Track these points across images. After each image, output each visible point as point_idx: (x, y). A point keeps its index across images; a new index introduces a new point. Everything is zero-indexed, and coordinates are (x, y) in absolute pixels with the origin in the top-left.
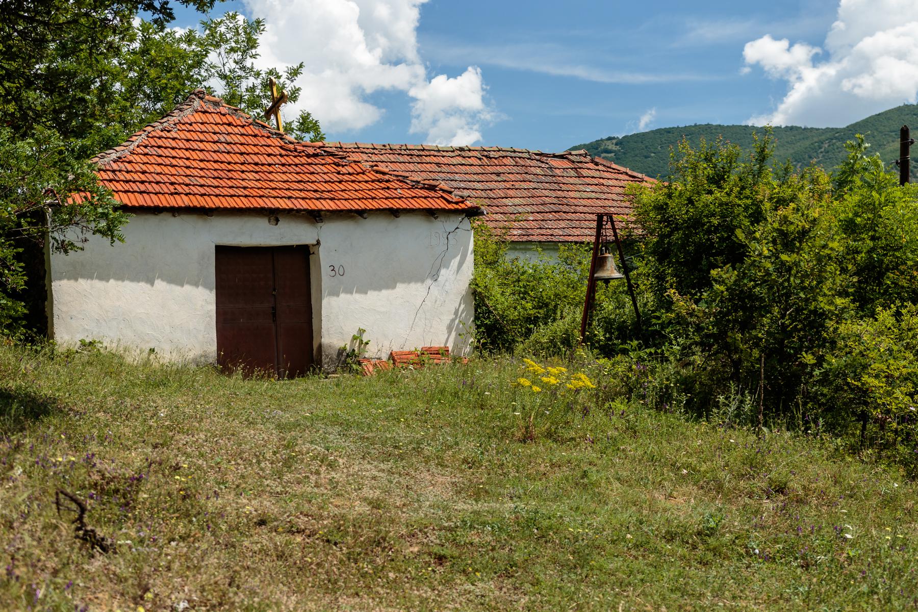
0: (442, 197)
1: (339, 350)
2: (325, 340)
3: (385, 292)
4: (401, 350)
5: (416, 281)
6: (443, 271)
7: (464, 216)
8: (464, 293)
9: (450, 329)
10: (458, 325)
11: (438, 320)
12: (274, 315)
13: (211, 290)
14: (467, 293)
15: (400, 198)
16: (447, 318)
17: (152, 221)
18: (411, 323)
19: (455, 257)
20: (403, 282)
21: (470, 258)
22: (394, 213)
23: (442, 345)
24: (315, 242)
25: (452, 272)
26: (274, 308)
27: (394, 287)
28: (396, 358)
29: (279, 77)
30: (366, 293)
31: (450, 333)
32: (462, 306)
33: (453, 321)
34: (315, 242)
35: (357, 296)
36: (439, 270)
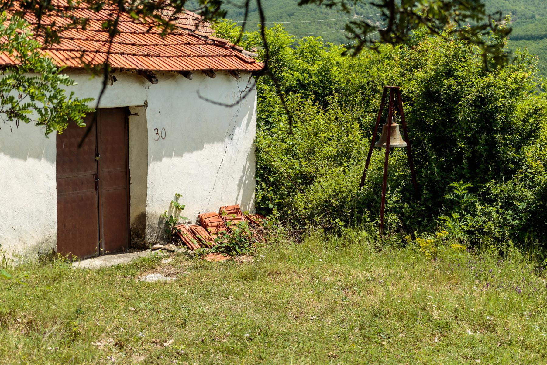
0: (236, 56)
1: (160, 218)
2: (149, 210)
3: (196, 154)
4: (206, 212)
5: (218, 141)
6: (237, 131)
7: (250, 75)
8: (249, 150)
9: (239, 186)
10: (245, 181)
11: (232, 179)
12: (97, 184)
13: (53, 163)
14: (251, 150)
15: (207, 57)
16: (238, 176)
17: (100, 103)
18: (213, 184)
19: (245, 116)
20: (209, 142)
21: (255, 117)
22: (210, 73)
23: (234, 204)
24: (143, 104)
25: (242, 131)
26: (97, 176)
27: (202, 148)
28: (207, 221)
29: (483, 34)
30: (182, 156)
31: (239, 190)
32: (248, 163)
33: (241, 178)
34: (143, 104)
35: (175, 159)
36: (233, 130)
